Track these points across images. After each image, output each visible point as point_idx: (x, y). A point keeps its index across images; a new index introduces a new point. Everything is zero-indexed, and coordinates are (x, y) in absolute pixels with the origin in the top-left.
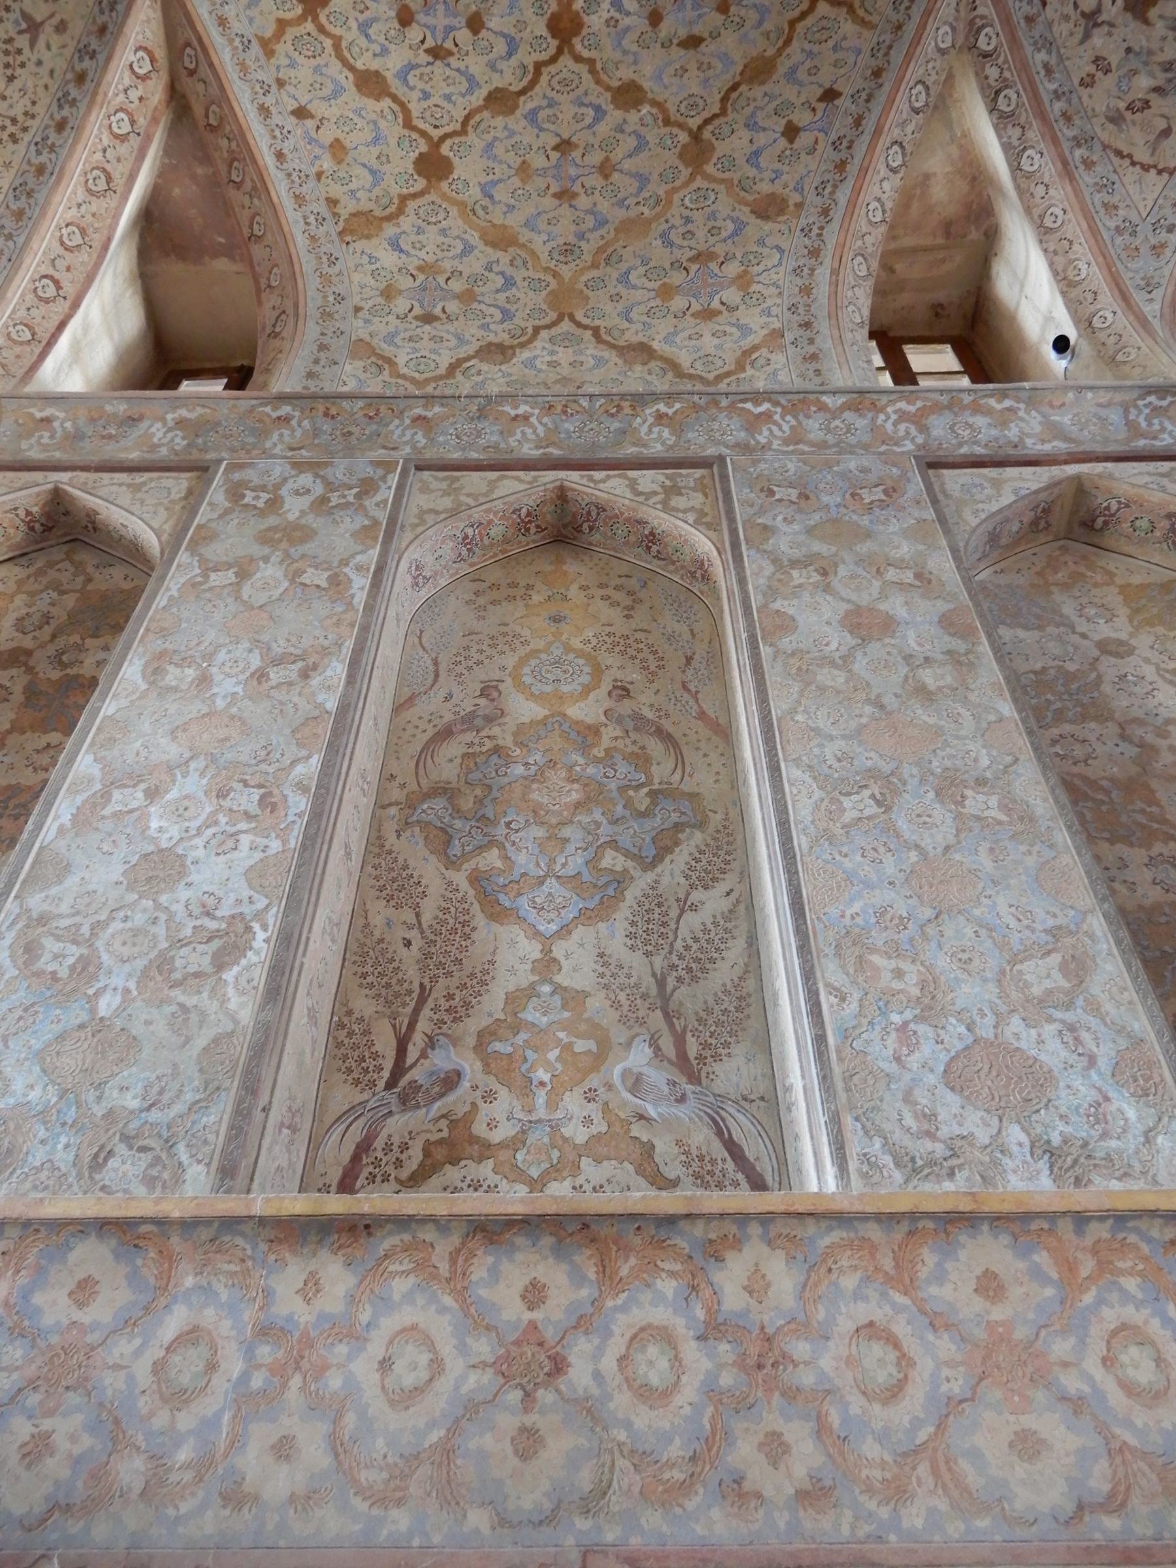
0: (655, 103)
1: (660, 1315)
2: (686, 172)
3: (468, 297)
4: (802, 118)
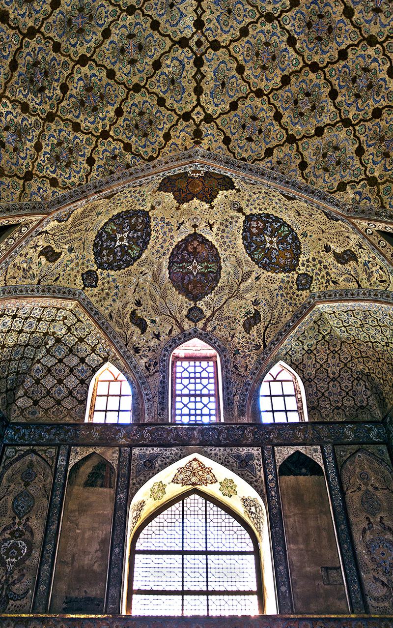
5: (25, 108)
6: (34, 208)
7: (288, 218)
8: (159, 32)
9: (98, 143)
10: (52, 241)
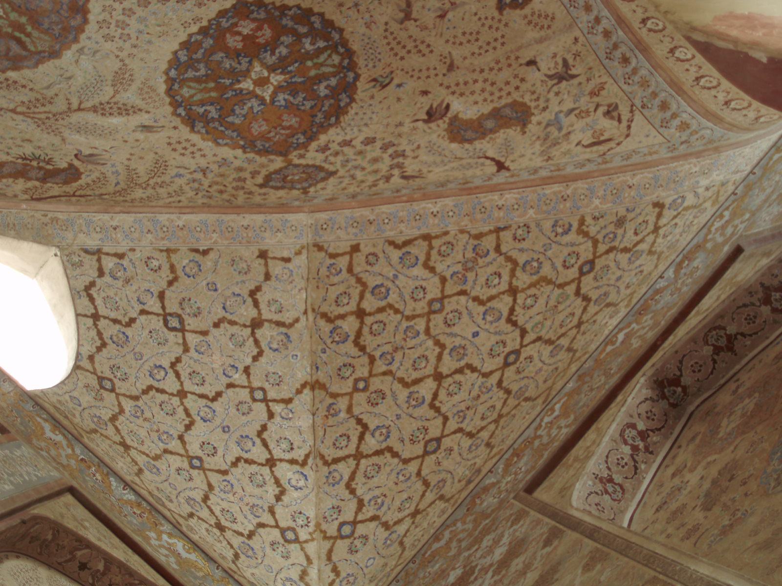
7: (363, 30)
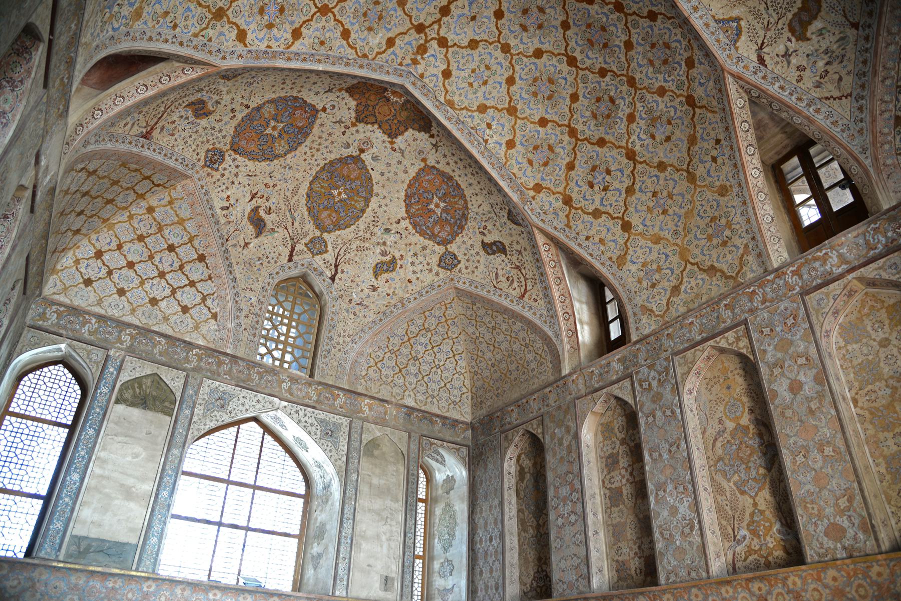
0: (671, 165)
1: (780, 590)
2: (692, 186)
3: (659, 269)
4: (714, 153)
5: (631, 118)
6: (720, 91)
8: (500, 6)
9: (631, 12)
10: (780, 26)
